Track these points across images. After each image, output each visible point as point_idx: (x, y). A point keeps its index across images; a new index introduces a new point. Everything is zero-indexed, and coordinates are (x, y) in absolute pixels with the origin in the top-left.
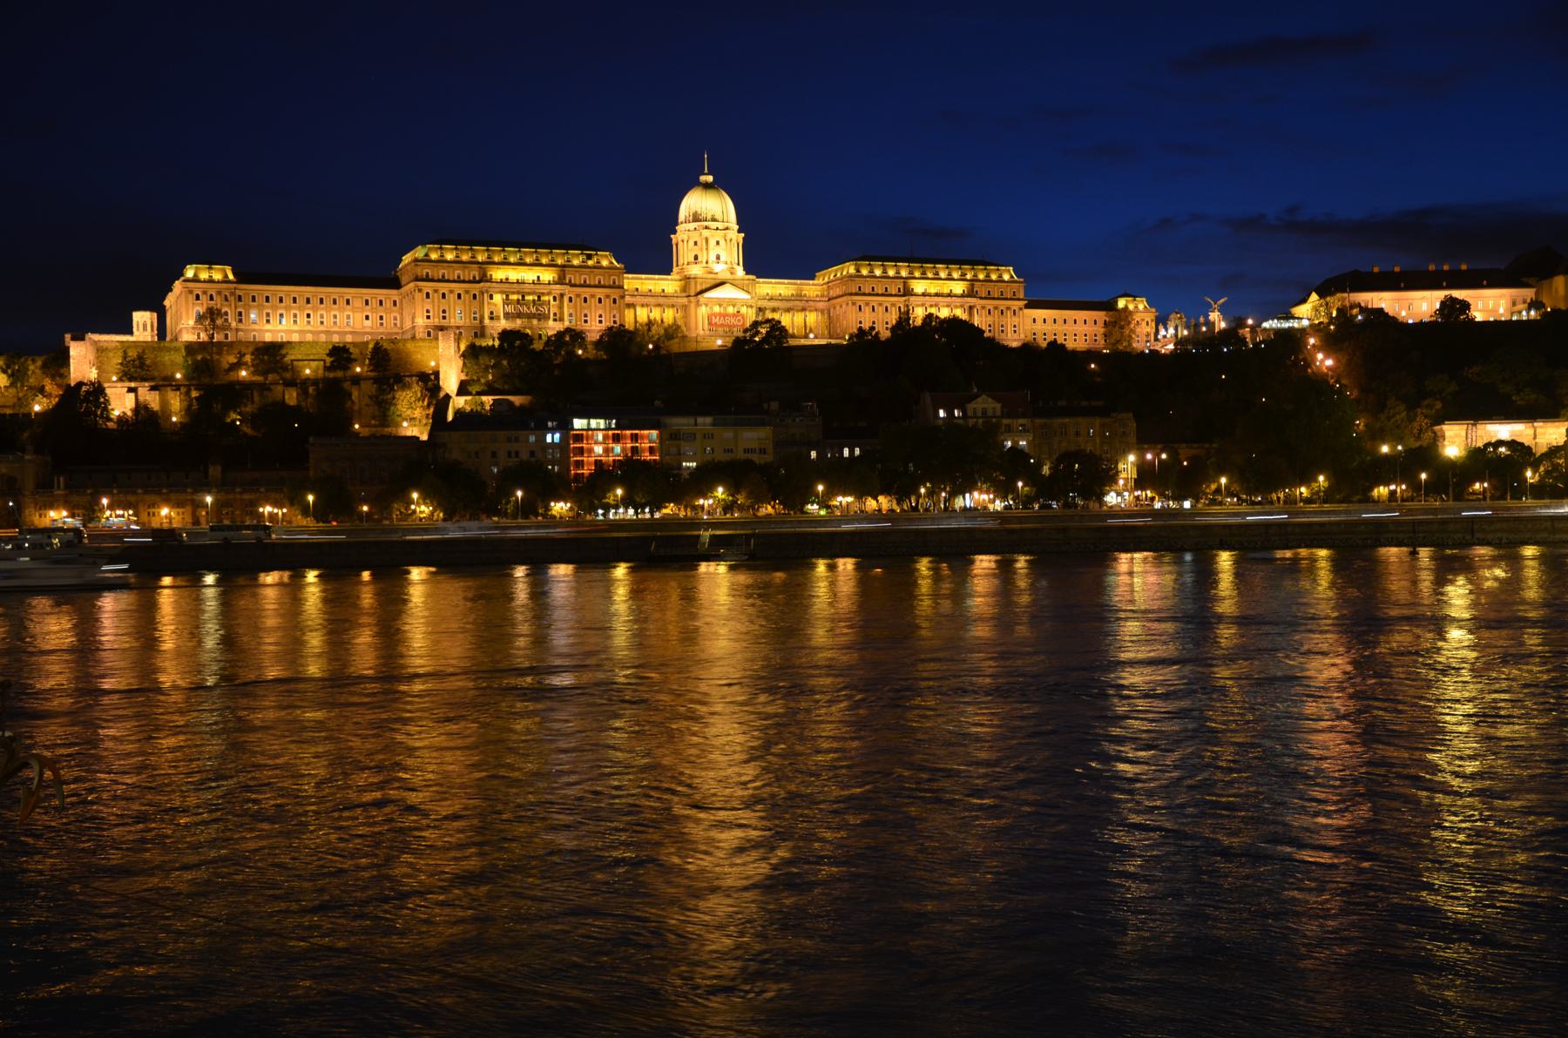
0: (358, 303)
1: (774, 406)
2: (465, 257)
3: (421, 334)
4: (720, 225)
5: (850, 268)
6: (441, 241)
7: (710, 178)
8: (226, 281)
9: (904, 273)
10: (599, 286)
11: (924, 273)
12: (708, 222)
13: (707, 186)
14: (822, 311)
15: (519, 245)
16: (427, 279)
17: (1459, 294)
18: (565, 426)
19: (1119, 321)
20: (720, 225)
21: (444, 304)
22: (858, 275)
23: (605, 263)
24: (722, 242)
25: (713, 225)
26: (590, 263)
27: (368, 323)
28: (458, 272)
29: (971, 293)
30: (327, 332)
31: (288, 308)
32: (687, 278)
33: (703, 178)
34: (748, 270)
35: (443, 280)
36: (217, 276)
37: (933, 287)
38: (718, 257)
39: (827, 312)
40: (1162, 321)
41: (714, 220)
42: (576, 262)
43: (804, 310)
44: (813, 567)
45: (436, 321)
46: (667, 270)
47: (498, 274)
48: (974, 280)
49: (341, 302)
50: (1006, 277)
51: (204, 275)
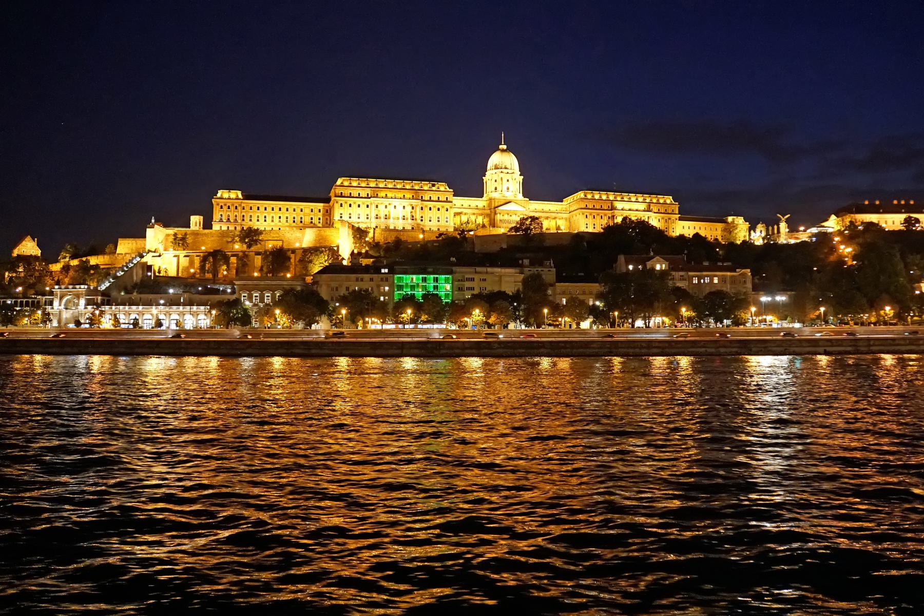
1: (526, 262)
2: (363, 185)
5: (581, 194)
7: (505, 147)
9: (611, 198)
10: (438, 201)
12: (504, 172)
13: (503, 151)
14: (566, 219)
16: (341, 196)
19: (730, 229)
20: (510, 171)
22: (586, 198)
23: (442, 189)
26: (434, 188)
32: (490, 199)
33: (501, 147)
34: (524, 196)
35: (350, 196)
39: (569, 220)
40: (752, 228)
41: (506, 168)
42: (426, 188)
43: (555, 218)
46: (481, 195)
50: (668, 202)
51: (226, 195)
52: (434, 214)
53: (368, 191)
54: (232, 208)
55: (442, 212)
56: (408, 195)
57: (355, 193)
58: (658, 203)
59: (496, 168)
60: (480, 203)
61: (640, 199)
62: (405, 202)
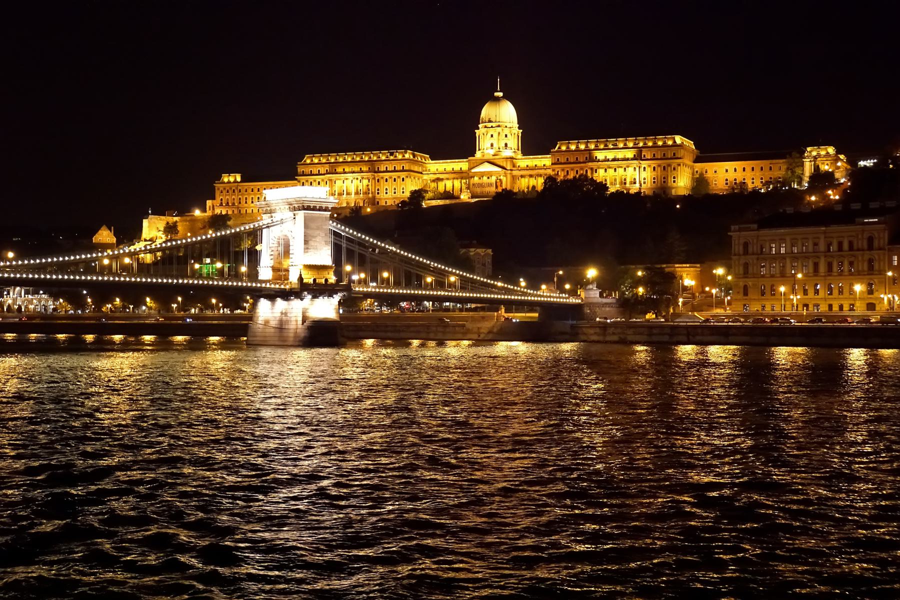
2: (324, 161)
4: (494, 125)
6: (313, 151)
7: (501, 94)
8: (235, 182)
9: (592, 146)
10: (395, 171)
11: (606, 145)
15: (354, 150)
20: (494, 125)
24: (495, 135)
25: (489, 125)
26: (392, 158)
29: (639, 157)
36: (232, 179)
37: (610, 155)
38: (492, 145)
41: (490, 121)
42: (384, 158)
48: (645, 147)
51: (226, 180)
52: (390, 186)
53: (327, 167)
54: (230, 192)
55: (438, 176)
56: (365, 169)
57: (315, 171)
58: (655, 146)
60: (461, 165)
61: (631, 145)
62: (358, 176)
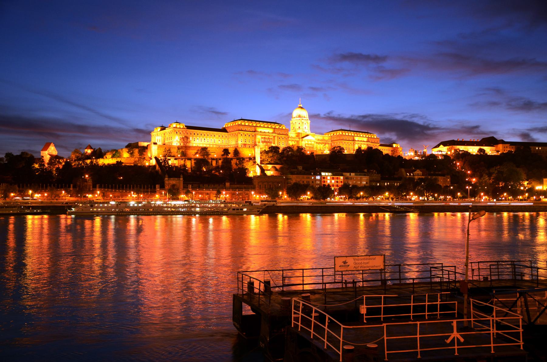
0: (217, 136)
2: (251, 125)
3: (240, 146)
9: (353, 135)
17: (482, 147)
18: (320, 175)
21: (245, 138)
23: (284, 128)
27: (219, 142)
28: (249, 129)
30: (209, 144)
31: (200, 137)
32: (299, 133)
44: (433, 215)
45: (244, 142)
47: (259, 129)
49: (213, 136)
51: (178, 126)
59: (300, 116)
